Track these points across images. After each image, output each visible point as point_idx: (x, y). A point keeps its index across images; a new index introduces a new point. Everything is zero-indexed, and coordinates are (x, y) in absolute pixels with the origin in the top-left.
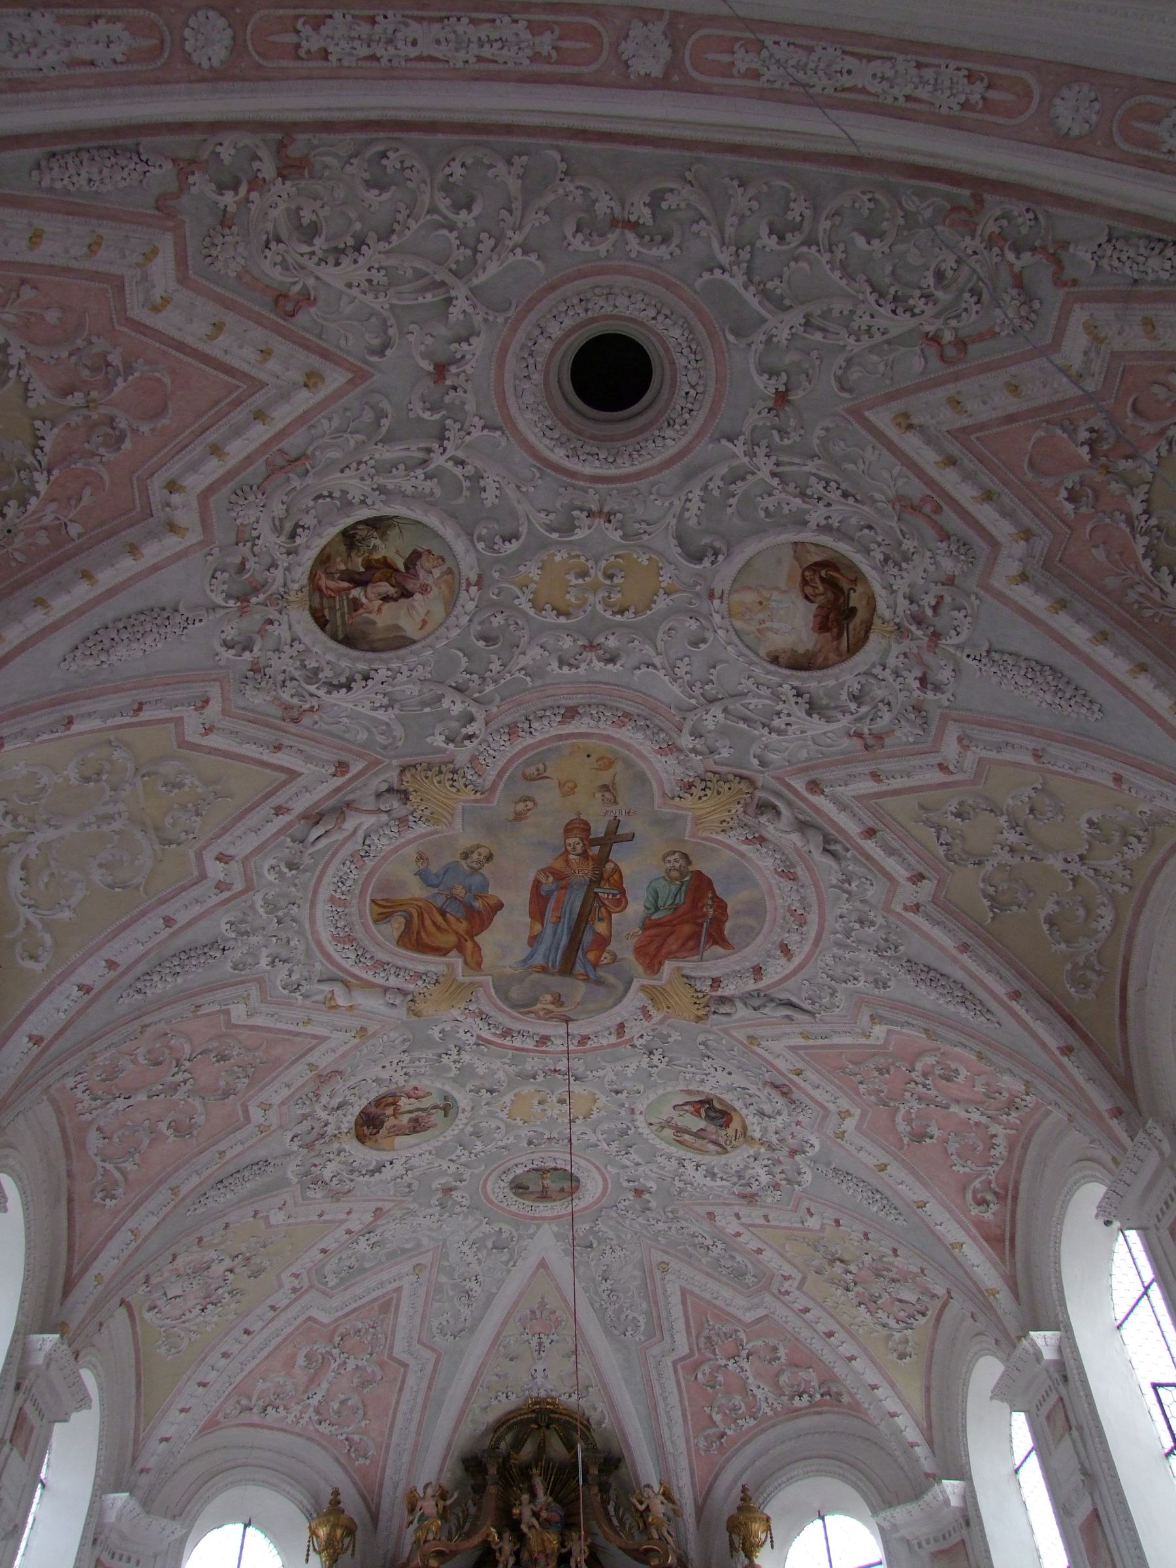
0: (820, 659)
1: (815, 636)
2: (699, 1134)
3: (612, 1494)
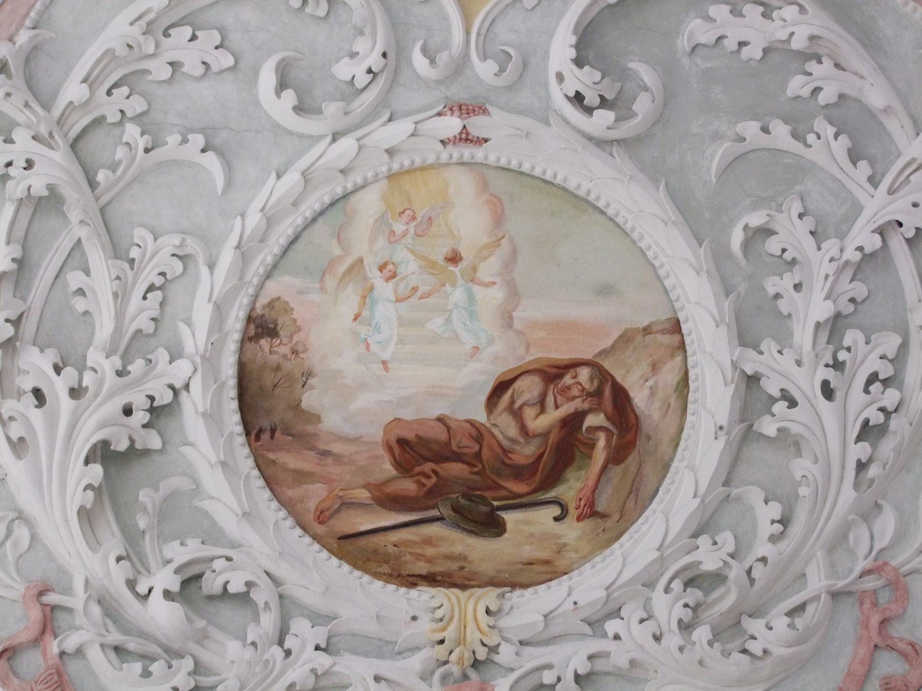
0: (291, 460)
1: (375, 433)
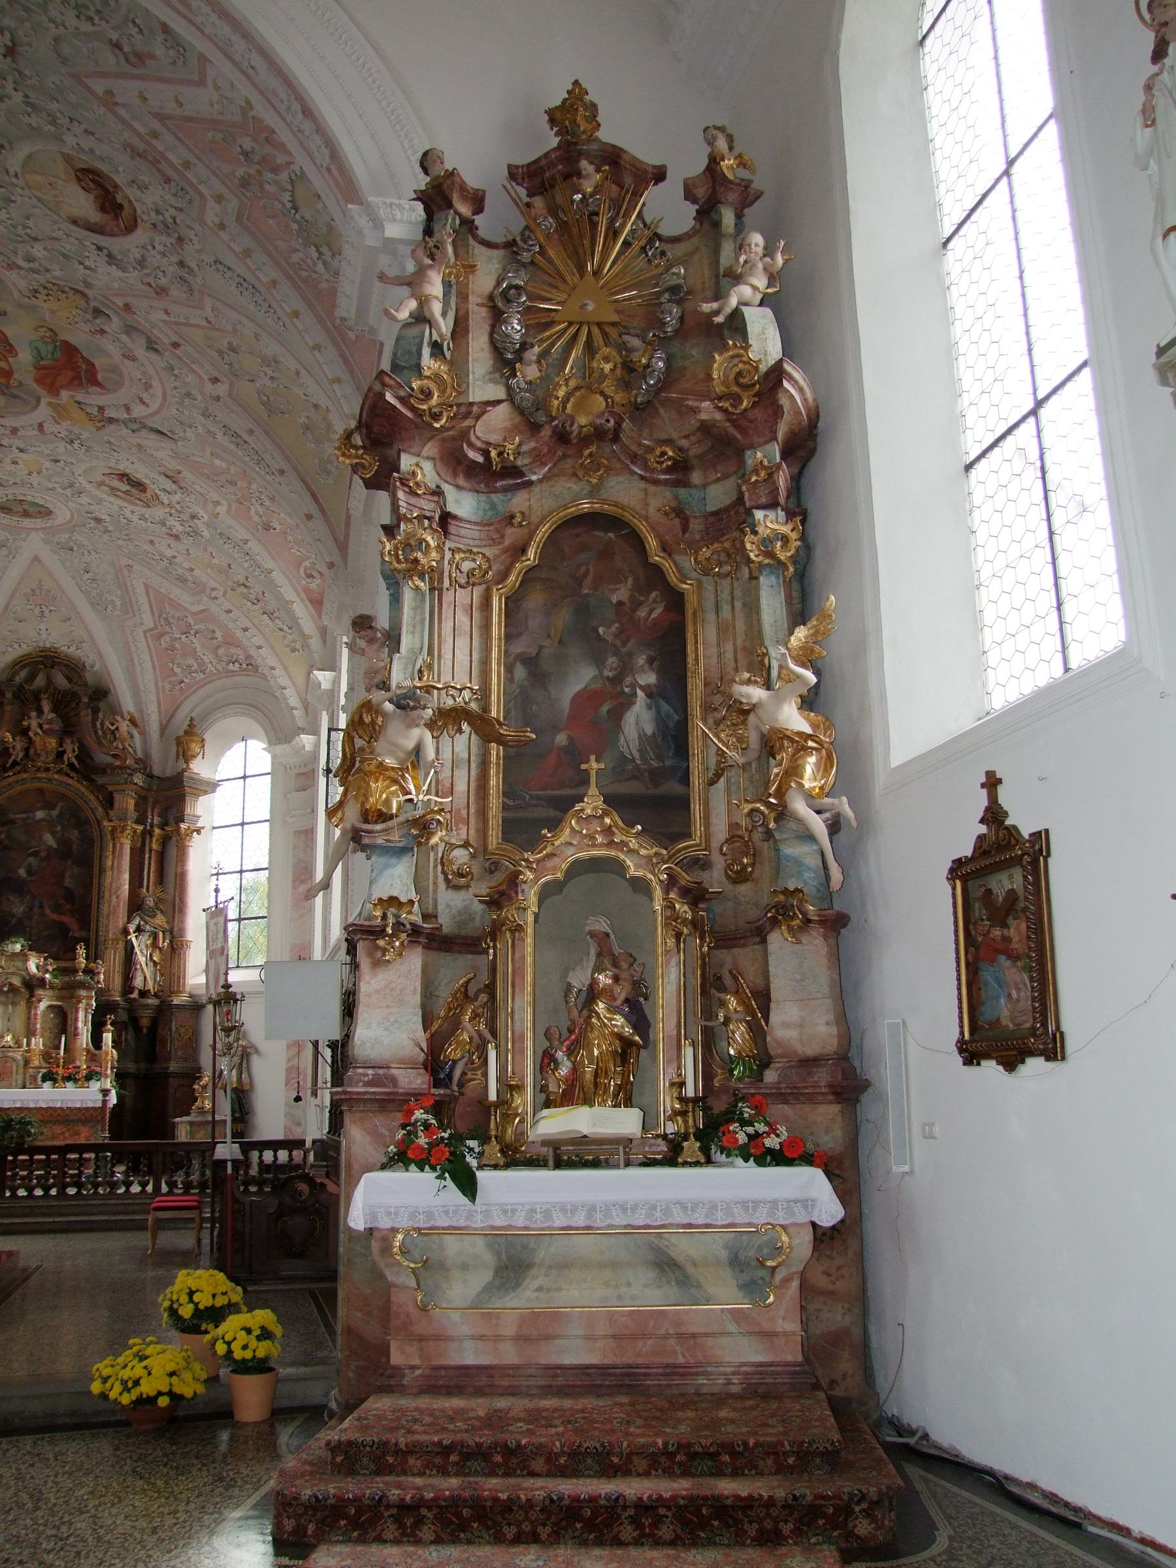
2: (125, 492)
3: (101, 715)
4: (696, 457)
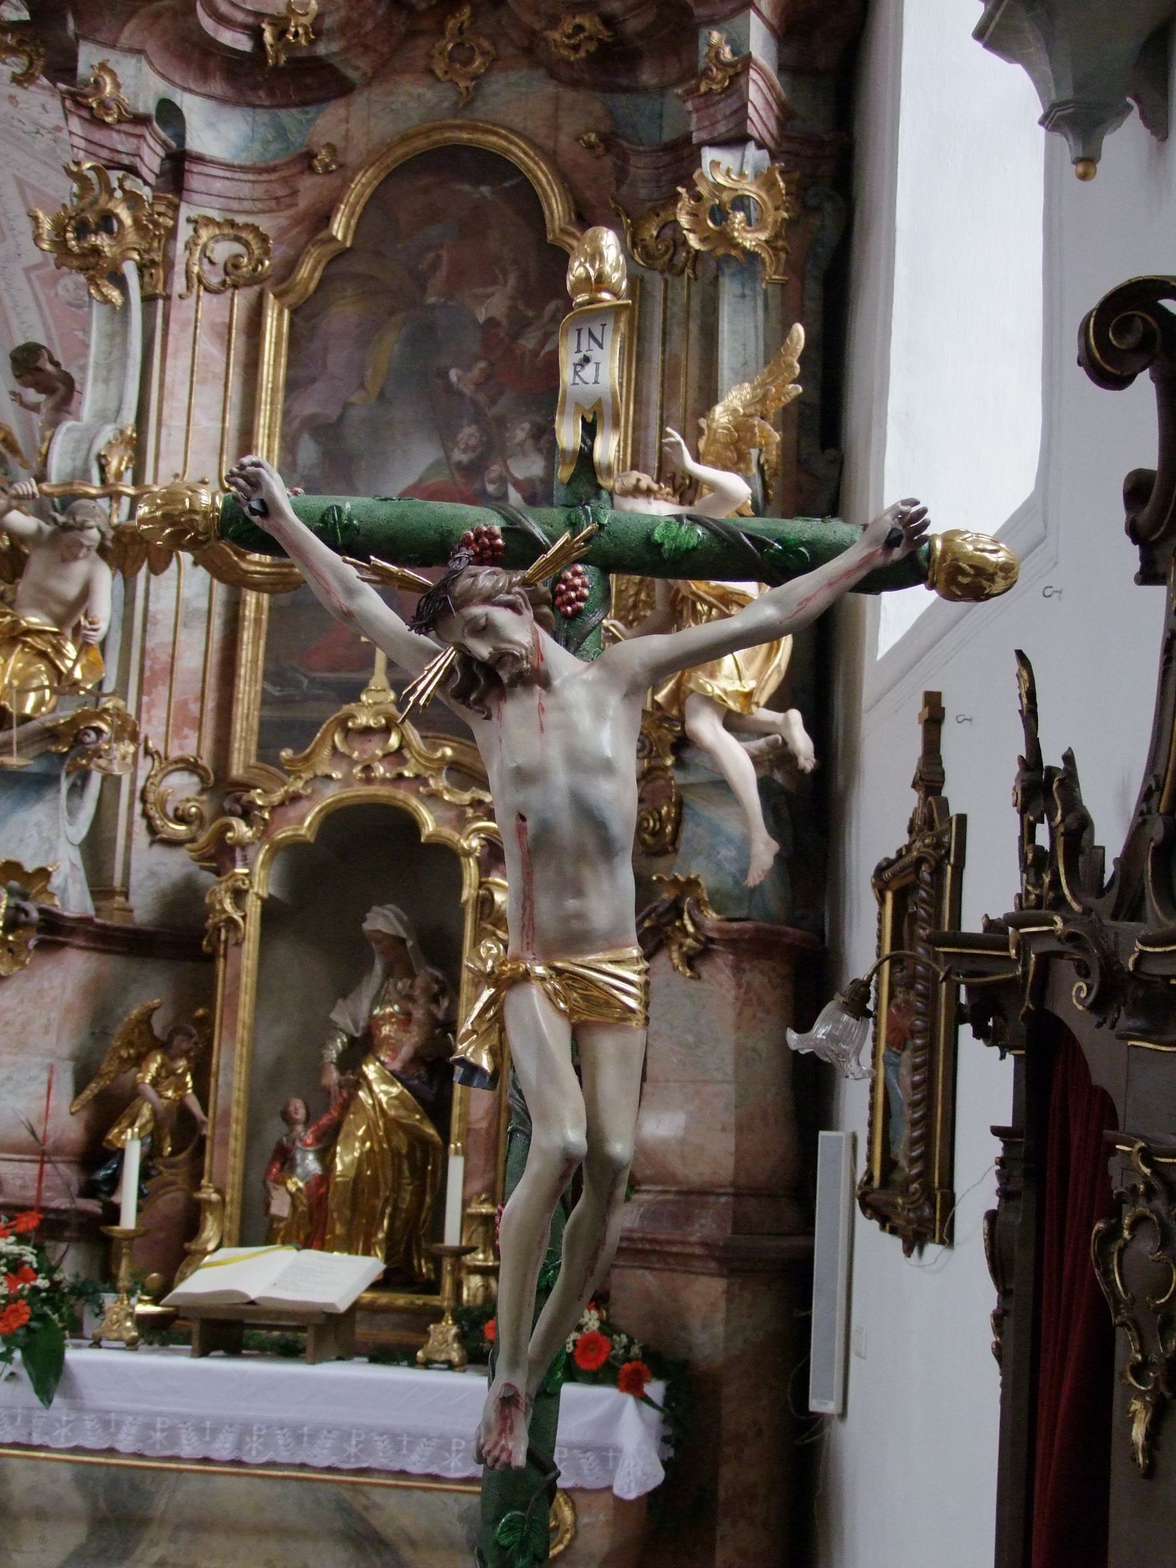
4: (639, 35)
